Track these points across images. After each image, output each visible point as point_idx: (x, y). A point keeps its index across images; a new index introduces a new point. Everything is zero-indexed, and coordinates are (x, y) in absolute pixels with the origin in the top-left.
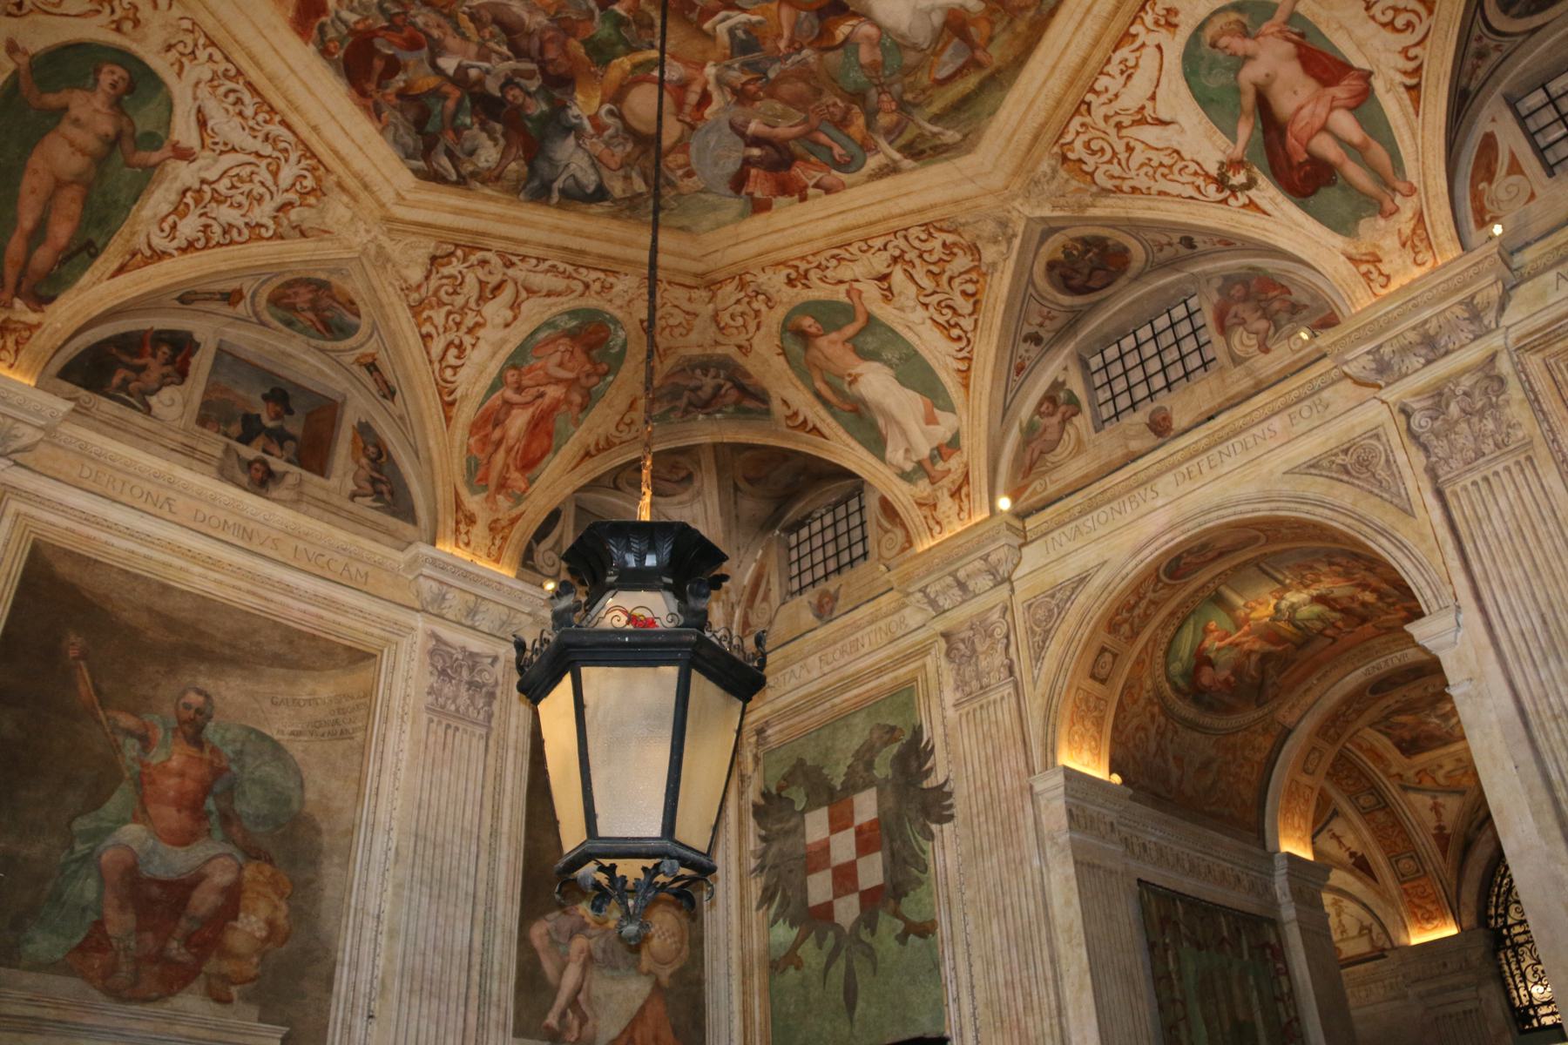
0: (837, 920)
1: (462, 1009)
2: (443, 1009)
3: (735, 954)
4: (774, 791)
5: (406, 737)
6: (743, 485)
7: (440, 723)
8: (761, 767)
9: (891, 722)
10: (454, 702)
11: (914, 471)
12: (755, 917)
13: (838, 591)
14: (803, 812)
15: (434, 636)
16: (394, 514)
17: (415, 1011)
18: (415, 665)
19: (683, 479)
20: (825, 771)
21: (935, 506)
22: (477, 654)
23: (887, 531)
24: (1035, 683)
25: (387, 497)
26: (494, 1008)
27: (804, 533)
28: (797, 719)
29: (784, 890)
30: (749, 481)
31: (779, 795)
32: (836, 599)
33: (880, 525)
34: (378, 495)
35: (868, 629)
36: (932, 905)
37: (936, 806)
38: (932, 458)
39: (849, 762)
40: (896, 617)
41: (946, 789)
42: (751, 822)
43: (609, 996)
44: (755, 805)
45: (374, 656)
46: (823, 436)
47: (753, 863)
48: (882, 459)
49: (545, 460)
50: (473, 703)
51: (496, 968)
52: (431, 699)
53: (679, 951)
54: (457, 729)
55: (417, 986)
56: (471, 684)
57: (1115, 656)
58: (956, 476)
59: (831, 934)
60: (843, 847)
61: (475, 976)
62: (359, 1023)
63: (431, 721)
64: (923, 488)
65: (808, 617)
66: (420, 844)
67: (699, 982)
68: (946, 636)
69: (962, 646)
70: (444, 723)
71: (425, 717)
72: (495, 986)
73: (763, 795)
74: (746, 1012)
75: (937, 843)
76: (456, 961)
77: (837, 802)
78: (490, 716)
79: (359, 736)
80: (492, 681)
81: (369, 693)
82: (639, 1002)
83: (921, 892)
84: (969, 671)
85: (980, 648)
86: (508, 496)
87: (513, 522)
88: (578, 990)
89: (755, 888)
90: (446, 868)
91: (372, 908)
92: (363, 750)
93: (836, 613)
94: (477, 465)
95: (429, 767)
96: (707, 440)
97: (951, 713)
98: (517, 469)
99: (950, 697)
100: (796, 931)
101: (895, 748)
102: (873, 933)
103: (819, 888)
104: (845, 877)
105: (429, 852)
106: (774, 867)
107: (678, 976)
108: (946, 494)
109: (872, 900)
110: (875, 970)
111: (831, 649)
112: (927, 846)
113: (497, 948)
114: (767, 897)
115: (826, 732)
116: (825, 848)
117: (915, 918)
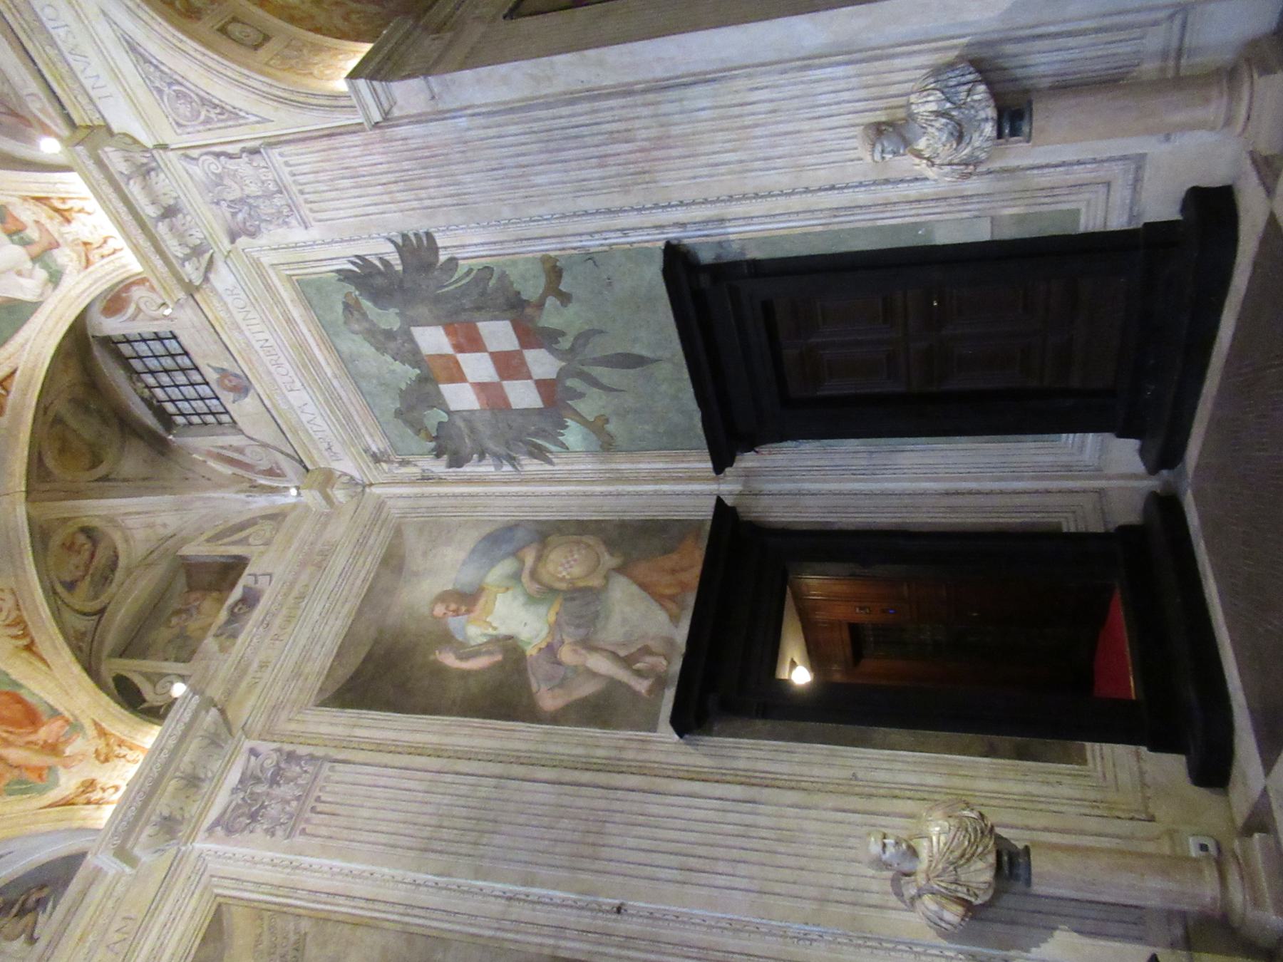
0: (554, 377)
1: (620, 794)
2: (618, 817)
3: (598, 489)
4: (432, 444)
5: (315, 861)
6: (101, 470)
7: (307, 821)
8: (411, 458)
9: (339, 308)
10: (288, 802)
11: (46, 267)
12: (561, 465)
13: (215, 369)
14: (449, 413)
15: (210, 830)
16: (66, 884)
17: (616, 854)
18: (240, 851)
19: (89, 537)
20: (403, 386)
21: (85, 244)
22: (243, 774)
23: (139, 310)
24: (264, 121)
25: (46, 891)
26: (625, 755)
27: (170, 408)
28: (356, 417)
29: (529, 435)
30: (96, 461)
31: (436, 438)
32: (223, 370)
33: (134, 318)
34: (41, 903)
35: (247, 333)
36: (527, 260)
37: (419, 252)
38: (25, 243)
39: (389, 359)
40: (229, 300)
41: (399, 241)
42: (468, 469)
43: (625, 621)
44: (450, 466)
45: (220, 905)
46: (13, 373)
47: (507, 468)
48: (34, 306)
49: (28, 698)
50: (293, 779)
51: (580, 751)
52: (280, 832)
53: (588, 546)
54: (318, 799)
55: (588, 851)
56: (274, 782)
57: (235, 20)
58: (43, 214)
59: (570, 383)
60: (478, 367)
61: (586, 777)
62: (625, 926)
63: (303, 832)
64: (65, 257)
65: (249, 402)
66: (437, 845)
67: (623, 525)
68: (233, 238)
69: (240, 217)
70: (308, 815)
71: (299, 840)
72: (601, 753)
73: (438, 456)
74: (656, 478)
75: (459, 254)
76: (566, 800)
77: (431, 377)
78: (312, 758)
79: (305, 925)
80: (275, 756)
81: (258, 911)
82: (634, 589)
83: (513, 274)
84: (265, 208)
85: (236, 194)
86: (67, 742)
87: (102, 733)
88: (615, 656)
89: (532, 466)
90: (464, 812)
91: (496, 907)
92: (322, 920)
93: (238, 372)
94: (20, 782)
95: (353, 835)
96: (21, 511)
97: (315, 233)
98: (35, 732)
99: (297, 234)
100: (569, 422)
101: (367, 304)
102: (563, 334)
103: (523, 395)
104: (509, 366)
105: (445, 833)
106: (507, 445)
107: (611, 545)
108: (66, 229)
109: (530, 335)
110: (601, 332)
111: (278, 378)
112: (463, 266)
113: (560, 749)
114: (539, 453)
115: (364, 384)
116: (481, 387)
117: (542, 282)
